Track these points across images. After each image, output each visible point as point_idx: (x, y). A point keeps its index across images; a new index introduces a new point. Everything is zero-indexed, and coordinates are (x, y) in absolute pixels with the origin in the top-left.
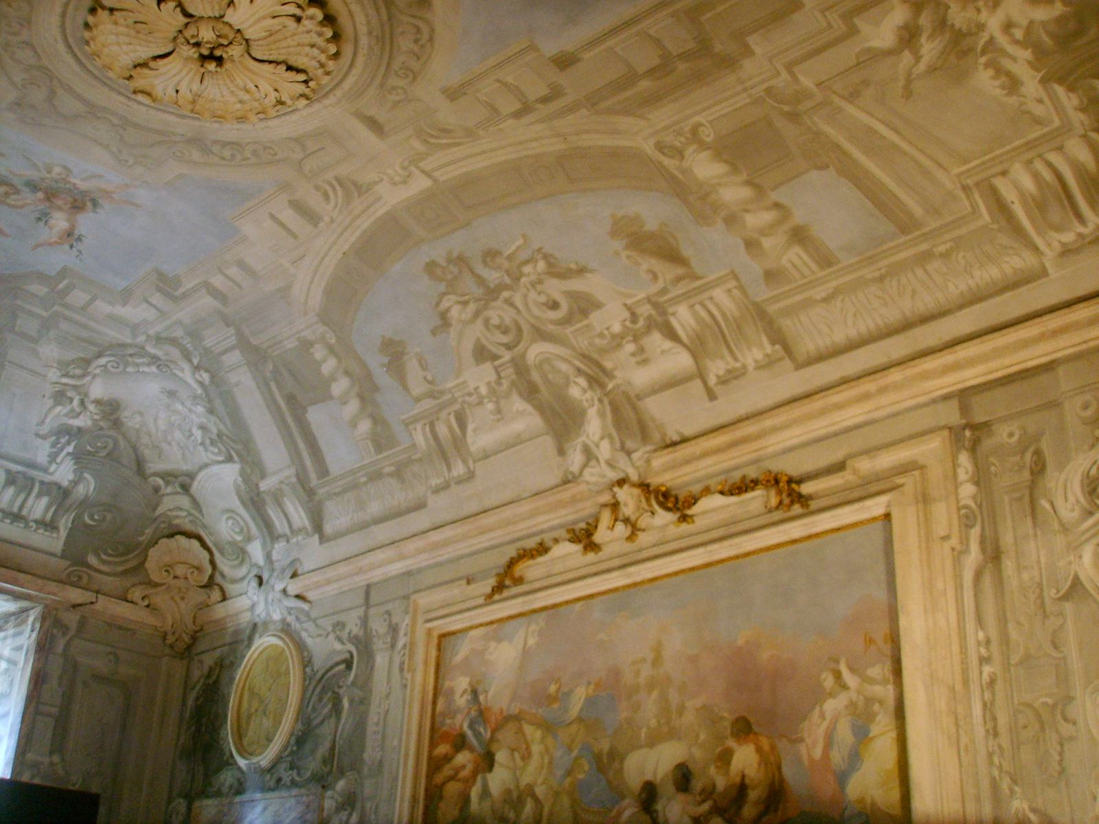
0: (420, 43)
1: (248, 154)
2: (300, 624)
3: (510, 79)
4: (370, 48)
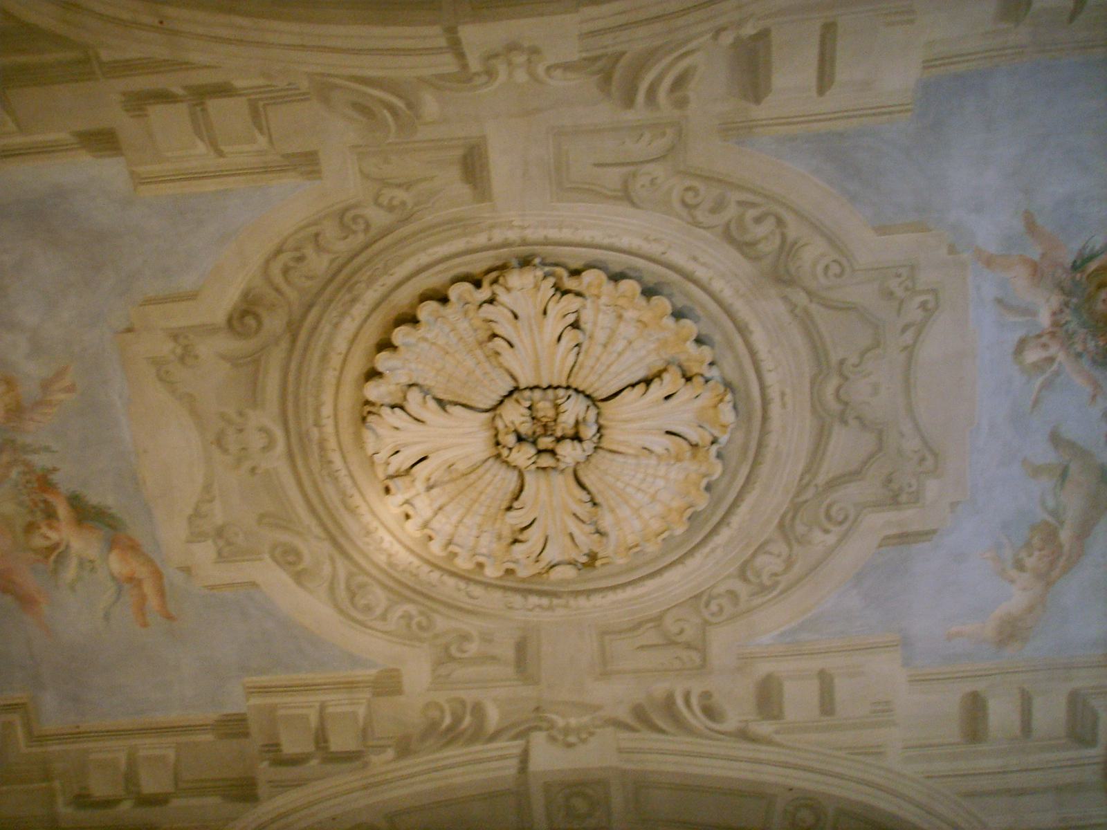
0: (298, 254)
1: (731, 212)
3: (201, 148)
4: (371, 281)
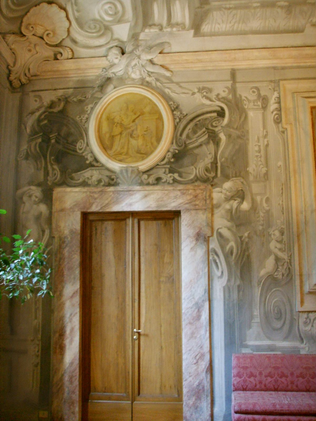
2: (161, 83)
